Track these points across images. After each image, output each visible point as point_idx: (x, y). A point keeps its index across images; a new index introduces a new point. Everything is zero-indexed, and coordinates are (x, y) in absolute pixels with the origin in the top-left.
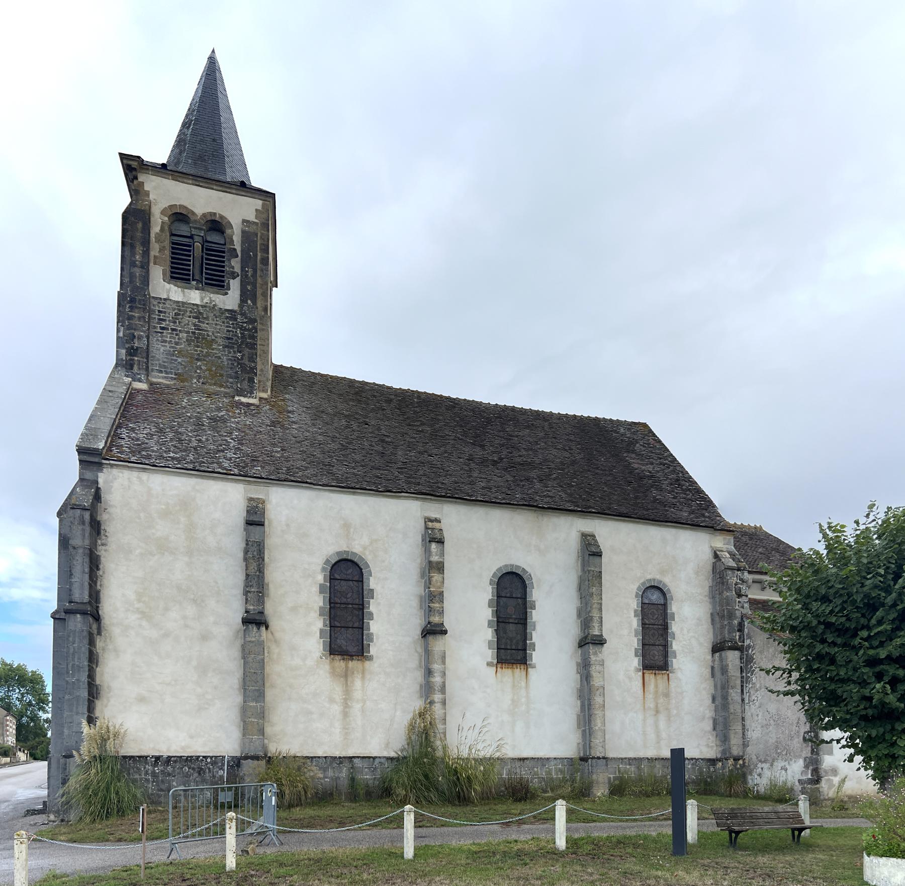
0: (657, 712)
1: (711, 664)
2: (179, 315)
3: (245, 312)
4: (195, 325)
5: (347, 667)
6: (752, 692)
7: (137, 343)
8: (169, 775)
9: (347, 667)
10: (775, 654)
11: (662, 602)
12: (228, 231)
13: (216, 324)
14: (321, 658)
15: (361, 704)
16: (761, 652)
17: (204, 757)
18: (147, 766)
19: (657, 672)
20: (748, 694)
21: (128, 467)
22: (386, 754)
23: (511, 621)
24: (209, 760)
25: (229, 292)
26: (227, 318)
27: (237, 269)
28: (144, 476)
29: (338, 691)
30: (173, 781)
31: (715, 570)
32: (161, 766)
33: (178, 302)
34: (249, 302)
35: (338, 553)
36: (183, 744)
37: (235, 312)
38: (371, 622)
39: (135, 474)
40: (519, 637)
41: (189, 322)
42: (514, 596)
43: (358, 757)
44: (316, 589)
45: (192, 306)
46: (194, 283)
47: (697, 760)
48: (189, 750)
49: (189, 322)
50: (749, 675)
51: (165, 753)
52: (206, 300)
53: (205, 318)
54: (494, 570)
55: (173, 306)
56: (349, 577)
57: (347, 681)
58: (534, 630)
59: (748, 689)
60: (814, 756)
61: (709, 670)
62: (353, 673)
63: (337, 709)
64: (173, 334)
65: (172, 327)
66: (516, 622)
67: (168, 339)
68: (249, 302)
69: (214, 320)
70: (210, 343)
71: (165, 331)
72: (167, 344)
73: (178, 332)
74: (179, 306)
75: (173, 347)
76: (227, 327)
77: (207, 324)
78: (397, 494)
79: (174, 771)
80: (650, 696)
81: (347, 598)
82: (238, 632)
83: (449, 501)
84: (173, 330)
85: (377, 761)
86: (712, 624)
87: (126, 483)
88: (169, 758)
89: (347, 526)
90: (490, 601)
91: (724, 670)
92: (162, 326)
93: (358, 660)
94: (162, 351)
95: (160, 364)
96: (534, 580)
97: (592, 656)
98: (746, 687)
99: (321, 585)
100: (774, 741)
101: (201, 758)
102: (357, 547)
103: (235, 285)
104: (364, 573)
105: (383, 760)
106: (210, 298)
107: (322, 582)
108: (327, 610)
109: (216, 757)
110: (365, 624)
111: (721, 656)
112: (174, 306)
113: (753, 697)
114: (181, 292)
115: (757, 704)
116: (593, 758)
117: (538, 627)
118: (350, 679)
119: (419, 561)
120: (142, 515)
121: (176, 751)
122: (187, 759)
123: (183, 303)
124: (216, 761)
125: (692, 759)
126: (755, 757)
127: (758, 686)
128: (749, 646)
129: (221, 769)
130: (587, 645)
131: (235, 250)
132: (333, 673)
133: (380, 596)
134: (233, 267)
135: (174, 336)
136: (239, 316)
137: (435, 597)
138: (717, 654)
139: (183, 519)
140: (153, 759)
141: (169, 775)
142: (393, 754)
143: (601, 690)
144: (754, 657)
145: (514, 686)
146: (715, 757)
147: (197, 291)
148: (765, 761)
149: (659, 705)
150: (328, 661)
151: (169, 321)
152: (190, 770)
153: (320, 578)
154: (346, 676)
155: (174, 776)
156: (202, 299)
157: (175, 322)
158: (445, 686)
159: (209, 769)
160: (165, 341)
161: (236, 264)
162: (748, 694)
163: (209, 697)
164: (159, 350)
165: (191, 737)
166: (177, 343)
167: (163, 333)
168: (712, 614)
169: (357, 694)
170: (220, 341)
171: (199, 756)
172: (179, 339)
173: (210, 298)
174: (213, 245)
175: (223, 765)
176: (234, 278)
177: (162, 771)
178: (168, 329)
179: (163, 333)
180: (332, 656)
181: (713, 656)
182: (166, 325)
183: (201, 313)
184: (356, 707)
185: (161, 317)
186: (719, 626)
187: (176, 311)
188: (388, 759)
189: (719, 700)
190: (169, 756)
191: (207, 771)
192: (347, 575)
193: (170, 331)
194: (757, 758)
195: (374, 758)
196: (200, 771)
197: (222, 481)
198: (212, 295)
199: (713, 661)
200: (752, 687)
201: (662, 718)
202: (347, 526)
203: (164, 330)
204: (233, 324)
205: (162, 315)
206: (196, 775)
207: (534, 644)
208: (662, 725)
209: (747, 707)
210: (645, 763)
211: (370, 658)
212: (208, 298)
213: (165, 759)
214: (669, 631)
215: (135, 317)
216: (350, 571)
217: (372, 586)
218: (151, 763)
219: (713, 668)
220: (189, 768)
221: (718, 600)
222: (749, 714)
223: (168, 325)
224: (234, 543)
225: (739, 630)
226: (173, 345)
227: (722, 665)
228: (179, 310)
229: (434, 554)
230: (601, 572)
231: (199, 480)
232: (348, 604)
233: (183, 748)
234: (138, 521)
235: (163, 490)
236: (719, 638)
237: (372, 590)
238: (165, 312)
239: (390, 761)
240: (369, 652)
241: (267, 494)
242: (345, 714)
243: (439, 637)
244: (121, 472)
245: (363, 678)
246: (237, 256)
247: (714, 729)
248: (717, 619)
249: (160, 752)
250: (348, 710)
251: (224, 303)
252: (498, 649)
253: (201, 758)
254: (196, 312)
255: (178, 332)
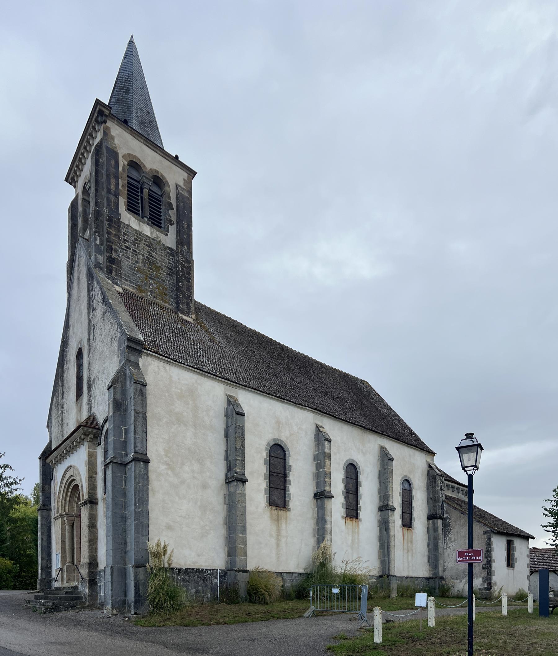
0: (408, 551)
1: (427, 526)
2: (137, 240)
3: (184, 253)
4: (148, 252)
5: (278, 514)
6: (448, 543)
7: (114, 253)
8: (187, 581)
9: (278, 514)
10: (465, 523)
11: (408, 489)
12: (166, 188)
13: (162, 256)
14: (266, 508)
15: (286, 539)
16: (455, 522)
17: (206, 570)
18: (173, 575)
19: (408, 528)
20: (446, 543)
21: (158, 358)
22: (297, 571)
23: (351, 492)
24: (209, 572)
25: (168, 234)
26: (168, 253)
27: (174, 218)
28: (168, 367)
29: (274, 528)
30: (189, 586)
31: (429, 475)
32: (182, 575)
33: (136, 231)
34: (185, 246)
35: (274, 439)
36: (194, 560)
37: (173, 250)
38: (290, 486)
39: (161, 364)
40: (354, 502)
41: (144, 248)
42: (352, 478)
43: (285, 572)
44: (262, 461)
45: (146, 237)
46: (146, 219)
47: (423, 578)
48: (197, 565)
49: (144, 248)
50: (447, 533)
51: (184, 567)
52: (154, 235)
53: (154, 249)
54: (345, 461)
55: (133, 232)
56: (278, 456)
57: (278, 523)
58: (361, 499)
59: (446, 541)
60: (489, 576)
61: (426, 529)
62: (281, 519)
63: (273, 541)
64: (134, 254)
65: (133, 248)
66: (353, 493)
67: (130, 257)
68: (185, 246)
69: (160, 252)
70: (158, 269)
71: (128, 250)
72: (130, 260)
73: (137, 254)
74: (137, 234)
75: (134, 264)
76: (169, 260)
77: (156, 253)
78: (304, 407)
79: (189, 579)
80: (405, 542)
81: (277, 470)
82: (222, 485)
83: (327, 417)
84: (134, 251)
85: (294, 575)
86: (428, 504)
87: (156, 369)
88: (187, 569)
89: (278, 422)
90: (343, 479)
91: (436, 530)
92: (126, 245)
93: (284, 510)
94: (126, 264)
95: (125, 274)
96: (361, 470)
97: (390, 517)
98: (445, 539)
99: (265, 459)
100: (463, 569)
101: (205, 570)
102: (284, 437)
103: (172, 229)
104: (287, 454)
105: (296, 575)
106: (157, 234)
107: (266, 457)
108: (268, 476)
109: (213, 570)
110: (287, 488)
111: (433, 522)
112: (134, 232)
113: (449, 545)
114: (137, 223)
115: (452, 549)
116: (391, 576)
117: (363, 497)
118: (280, 522)
119: (312, 450)
120: (167, 394)
121: (190, 565)
122: (197, 570)
123: (139, 232)
124: (213, 572)
125: (421, 577)
126: (450, 577)
127: (453, 539)
128: (447, 518)
129: (216, 578)
130: (388, 511)
131: (171, 204)
132: (271, 517)
133: (294, 470)
134: (170, 217)
135: (135, 255)
136: (180, 256)
137: (327, 475)
138: (431, 521)
139: (191, 402)
140: (177, 570)
141: (187, 581)
142: (302, 571)
143: (394, 536)
144: (451, 524)
145: (353, 531)
146: (428, 577)
147: (148, 226)
148: (456, 579)
149: (409, 547)
150: (269, 509)
151: (131, 242)
152: (199, 578)
153: (265, 454)
154: (278, 520)
155: (189, 583)
156: (152, 234)
157: (135, 245)
158: (332, 530)
159: (209, 578)
160: (129, 258)
161: (172, 214)
162: (446, 543)
163: (207, 528)
164: (126, 264)
165: (198, 555)
166: (137, 262)
167: (127, 250)
168: (427, 498)
169: (283, 533)
170: (164, 268)
171: (203, 569)
172: (138, 258)
173: (157, 234)
174: (153, 193)
175: (217, 575)
176: (171, 225)
177: (183, 579)
178: (130, 249)
179: (127, 250)
180: (271, 507)
181: (428, 522)
182: (129, 245)
183: (152, 244)
184: (283, 540)
185: (126, 238)
186: (432, 505)
187: (135, 237)
188: (300, 574)
189: (432, 546)
190: (186, 569)
191: (208, 579)
192: (277, 454)
193: (132, 251)
194: (451, 577)
195: (292, 573)
196: (204, 579)
197: (212, 380)
198: (158, 233)
199: (428, 524)
200: (448, 540)
201: (410, 554)
202: (278, 422)
203: (128, 249)
204: (172, 259)
205: (126, 236)
206: (202, 582)
207: (360, 507)
208: (410, 558)
209: (445, 550)
210: (404, 579)
211: (289, 510)
212: (155, 234)
213: (184, 571)
214: (412, 506)
215: (112, 233)
216: (279, 452)
217: (290, 464)
218: (176, 573)
219: (428, 528)
220: (198, 577)
221: (431, 491)
222: (446, 554)
223: (131, 246)
224: (220, 424)
225: (442, 509)
226: (134, 262)
227: (435, 527)
228: (138, 237)
229: (326, 448)
230: (393, 470)
231: (200, 377)
232: (278, 473)
233: (194, 563)
234: (164, 398)
235: (179, 379)
236: (432, 512)
237: (290, 466)
238: (128, 235)
239: (299, 575)
240: (289, 506)
241: (237, 394)
242: (278, 545)
243: (330, 500)
244: (153, 360)
245: (286, 522)
246: (172, 209)
247: (428, 562)
248: (431, 501)
249: (180, 565)
250: (279, 542)
251: (166, 241)
252: (346, 508)
253: (205, 570)
254: (148, 242)
255: (137, 254)
